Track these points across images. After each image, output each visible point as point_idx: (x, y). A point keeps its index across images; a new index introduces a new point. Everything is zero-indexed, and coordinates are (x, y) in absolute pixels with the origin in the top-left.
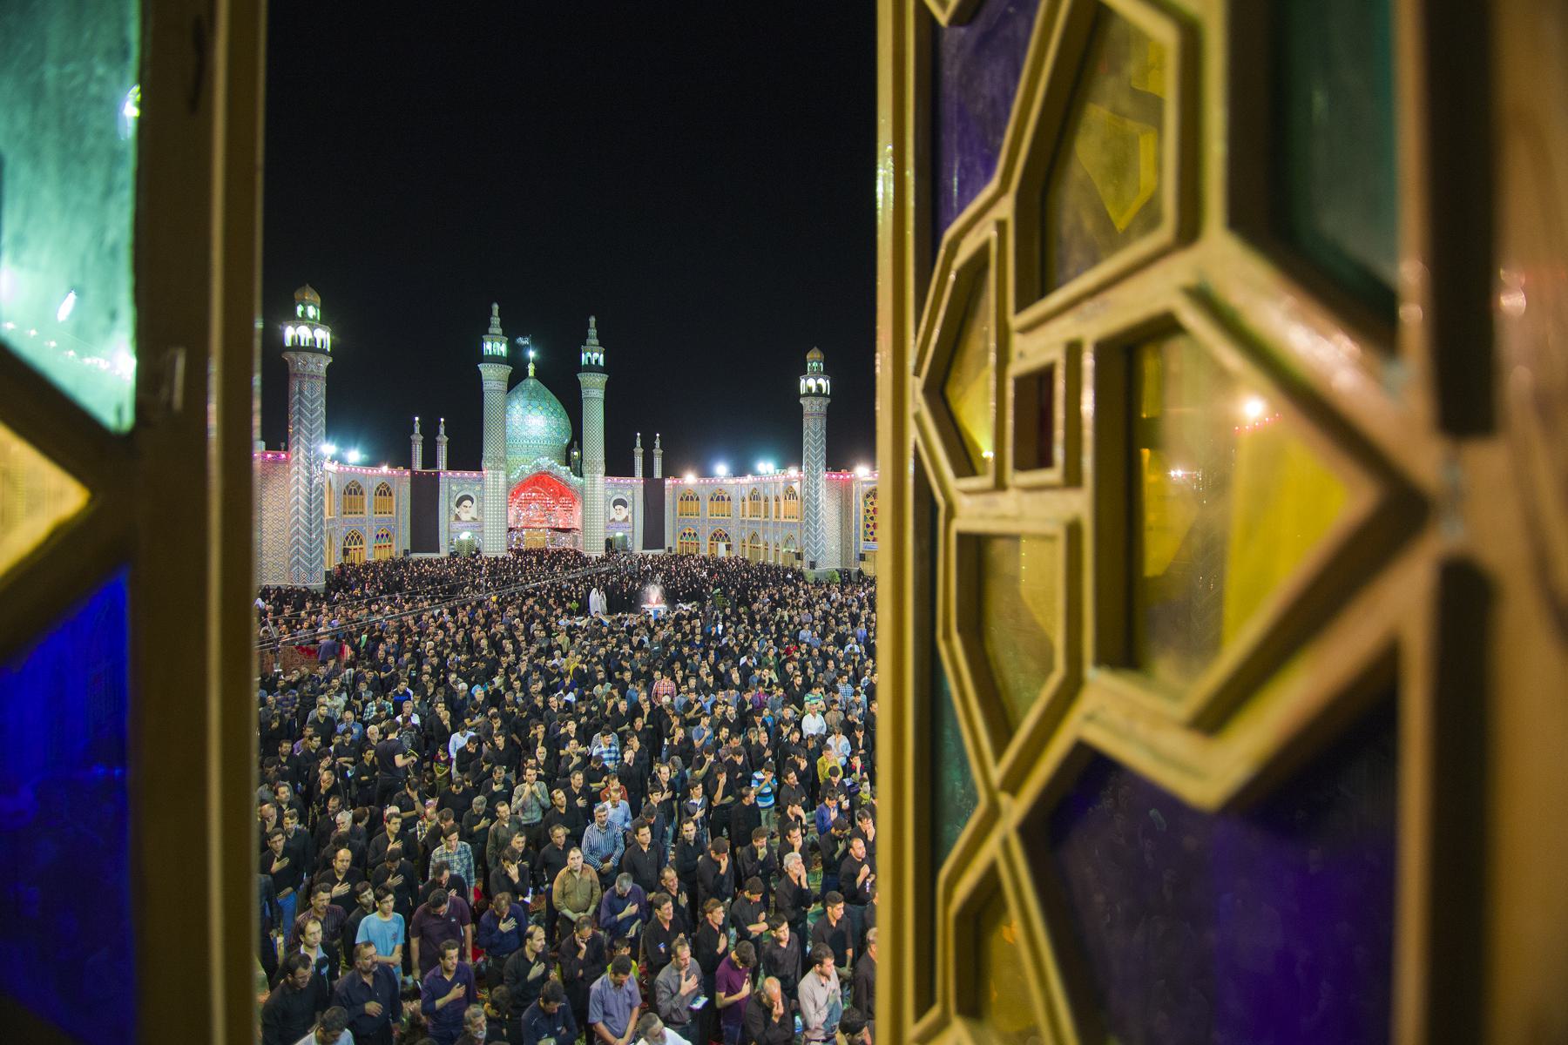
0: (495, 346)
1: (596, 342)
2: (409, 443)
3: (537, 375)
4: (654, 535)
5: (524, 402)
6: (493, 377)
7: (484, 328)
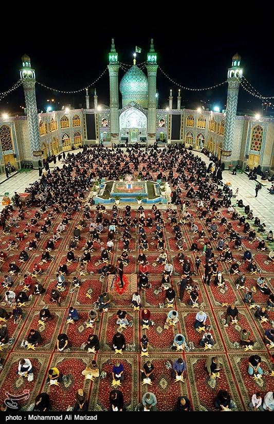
0: (113, 57)
1: (152, 50)
2: (85, 98)
3: (136, 64)
4: (176, 134)
5: (130, 77)
6: (112, 71)
7: (108, 50)
